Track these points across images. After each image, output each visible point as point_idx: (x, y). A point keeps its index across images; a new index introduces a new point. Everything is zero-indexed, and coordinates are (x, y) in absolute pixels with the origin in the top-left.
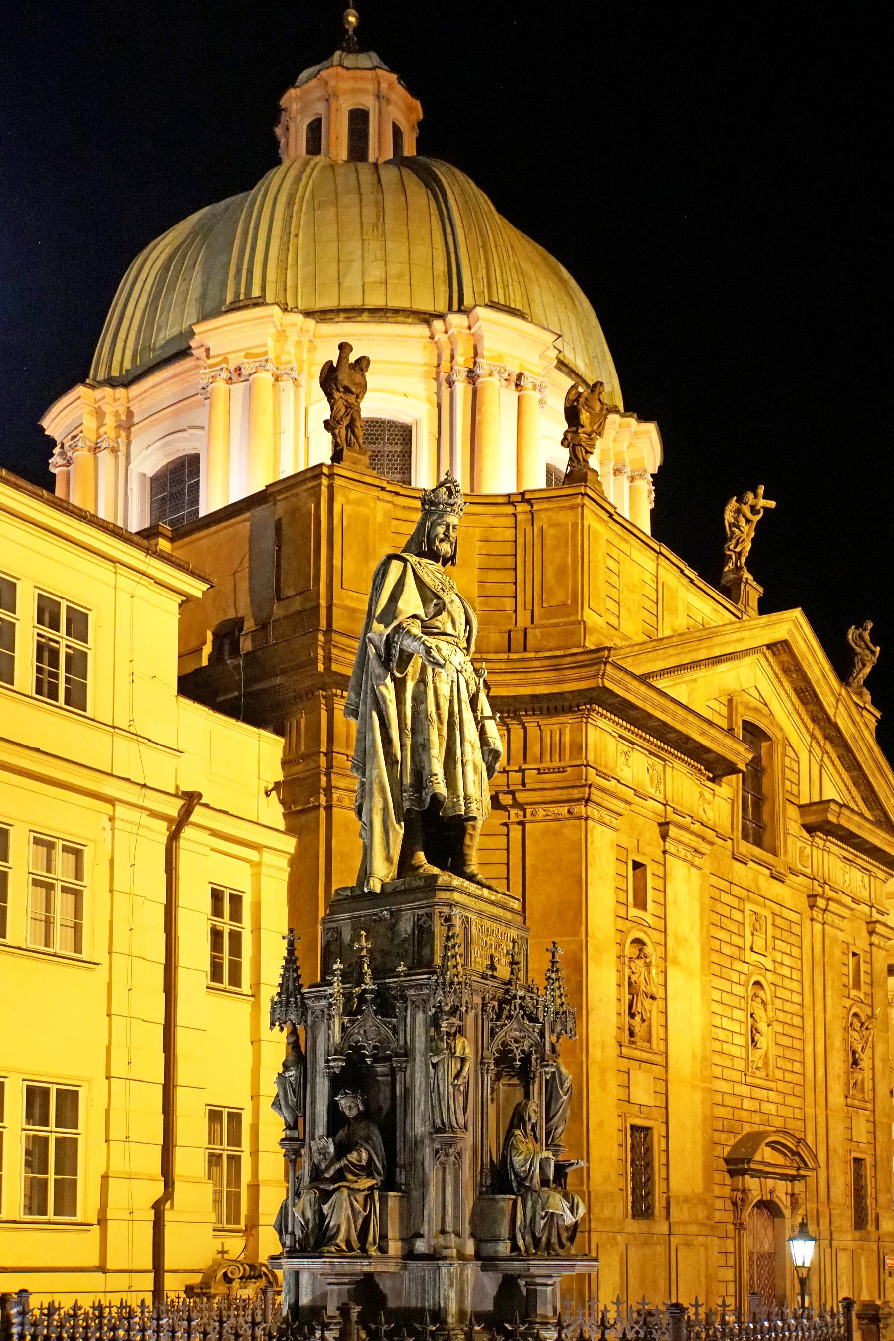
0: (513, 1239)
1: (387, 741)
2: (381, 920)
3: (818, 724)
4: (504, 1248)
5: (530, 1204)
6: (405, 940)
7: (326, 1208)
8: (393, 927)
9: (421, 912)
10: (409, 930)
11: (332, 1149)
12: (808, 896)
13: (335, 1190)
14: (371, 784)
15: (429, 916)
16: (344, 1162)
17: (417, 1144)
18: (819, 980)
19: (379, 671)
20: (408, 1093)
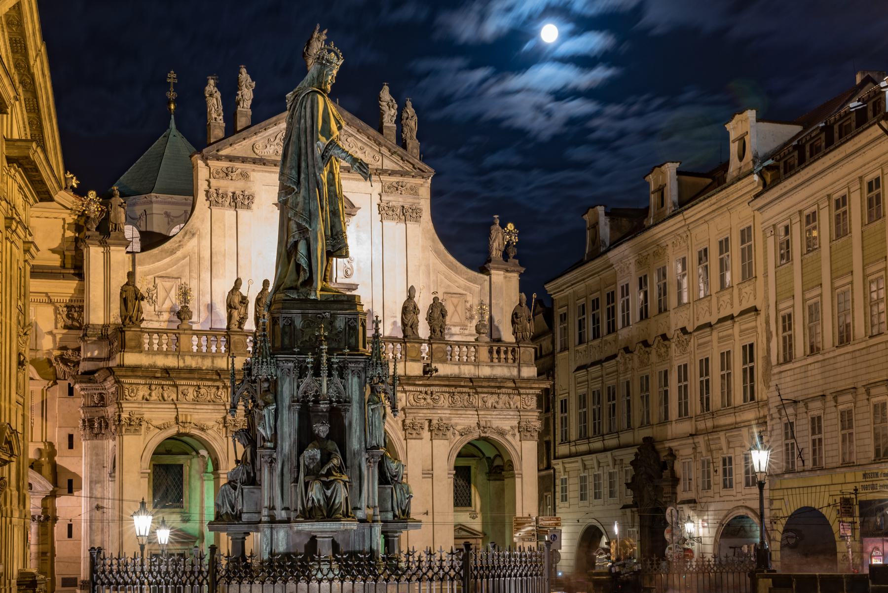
0: (393, 510)
1: (322, 208)
2: (323, 317)
3: (19, 70)
4: (390, 516)
5: (398, 491)
6: (340, 332)
7: (329, 493)
8: (331, 323)
9: (350, 317)
10: (342, 327)
11: (319, 457)
12: (6, 218)
13: (332, 482)
14: (316, 233)
15: (356, 320)
16: (331, 465)
17: (356, 454)
18: (8, 289)
19: (321, 164)
20: (350, 424)
